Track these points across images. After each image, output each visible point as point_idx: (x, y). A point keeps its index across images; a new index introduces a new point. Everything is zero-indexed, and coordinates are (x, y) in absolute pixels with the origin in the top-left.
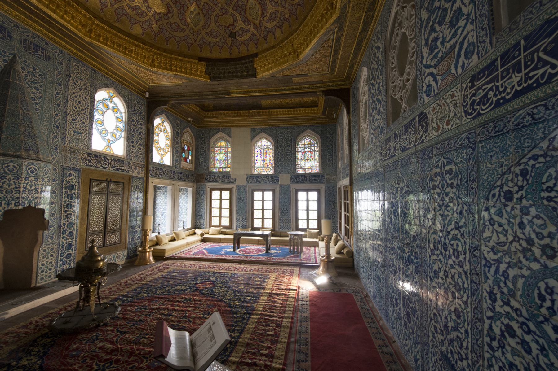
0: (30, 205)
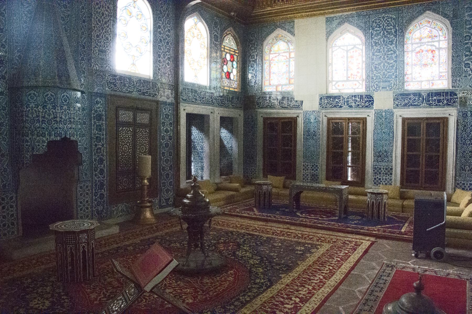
0: (66, 136)
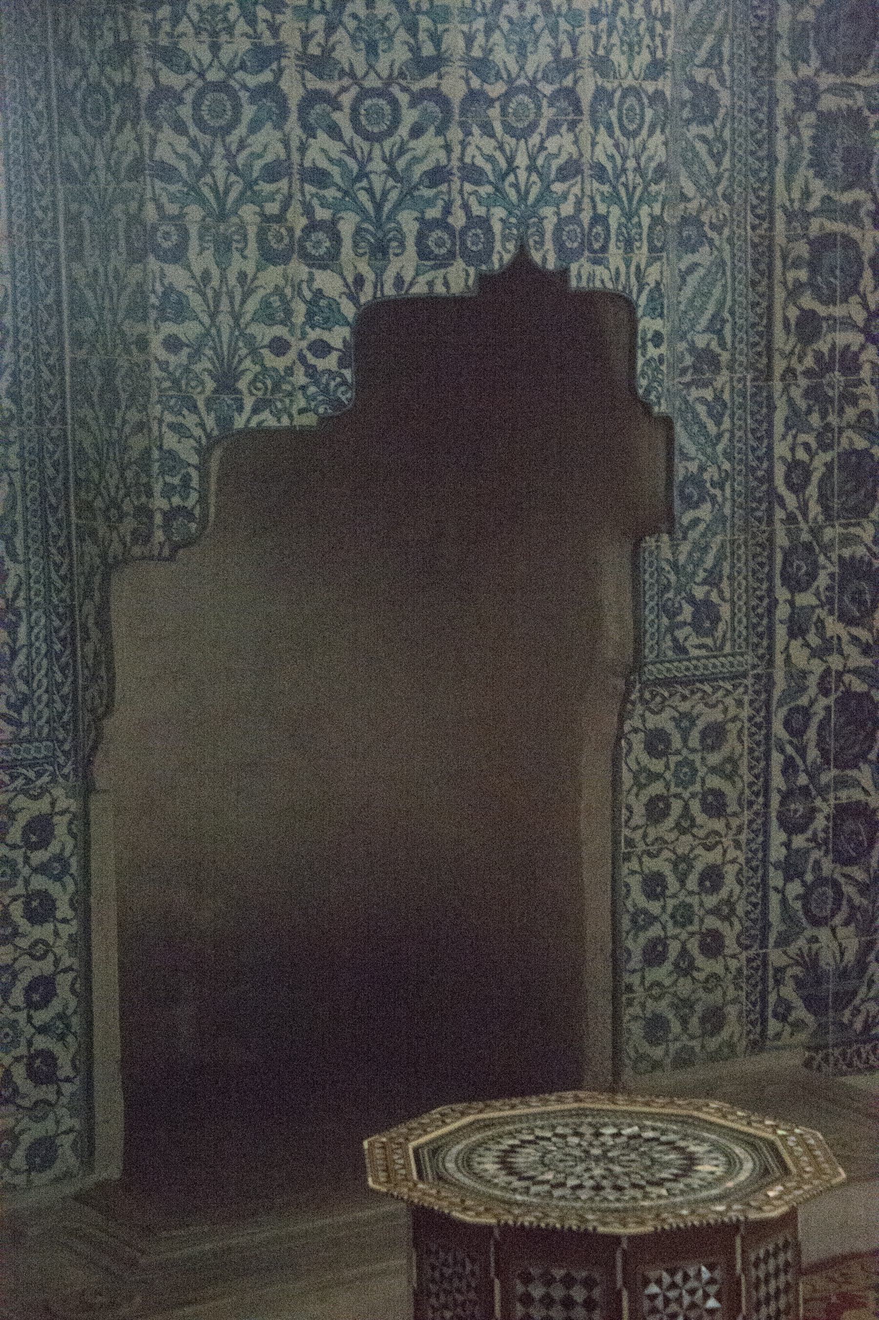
0: (522, 249)
